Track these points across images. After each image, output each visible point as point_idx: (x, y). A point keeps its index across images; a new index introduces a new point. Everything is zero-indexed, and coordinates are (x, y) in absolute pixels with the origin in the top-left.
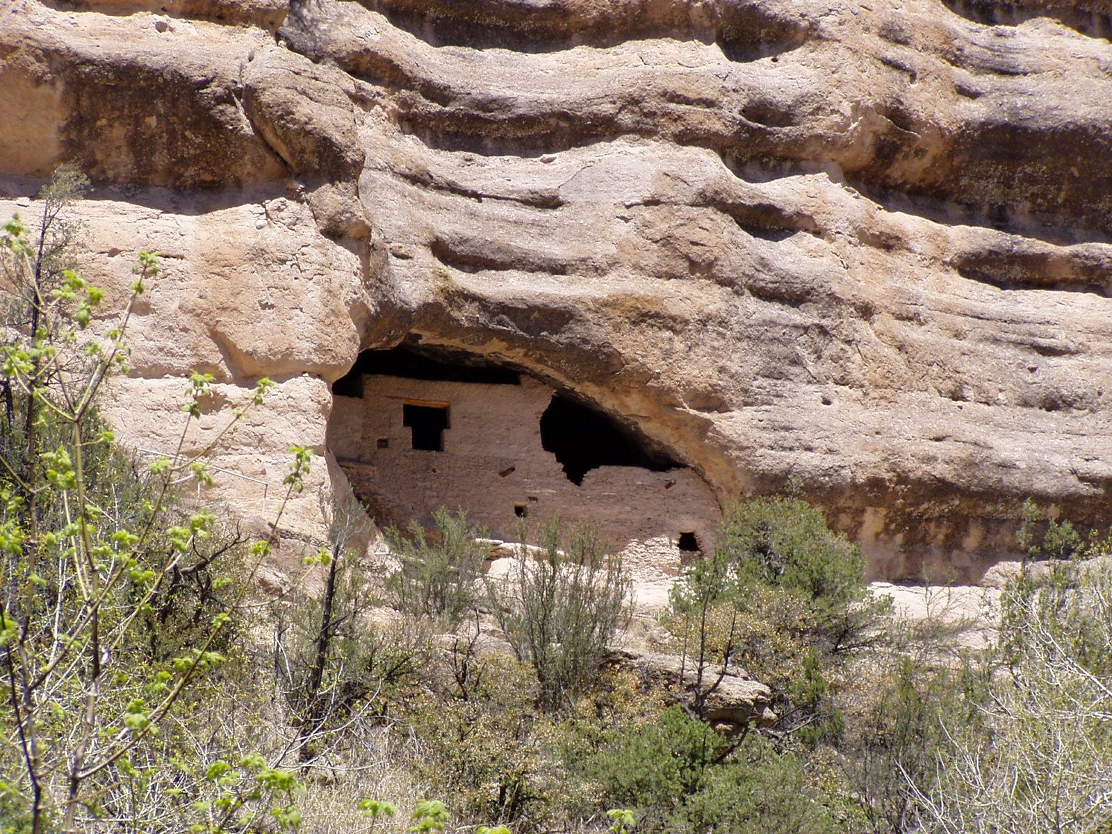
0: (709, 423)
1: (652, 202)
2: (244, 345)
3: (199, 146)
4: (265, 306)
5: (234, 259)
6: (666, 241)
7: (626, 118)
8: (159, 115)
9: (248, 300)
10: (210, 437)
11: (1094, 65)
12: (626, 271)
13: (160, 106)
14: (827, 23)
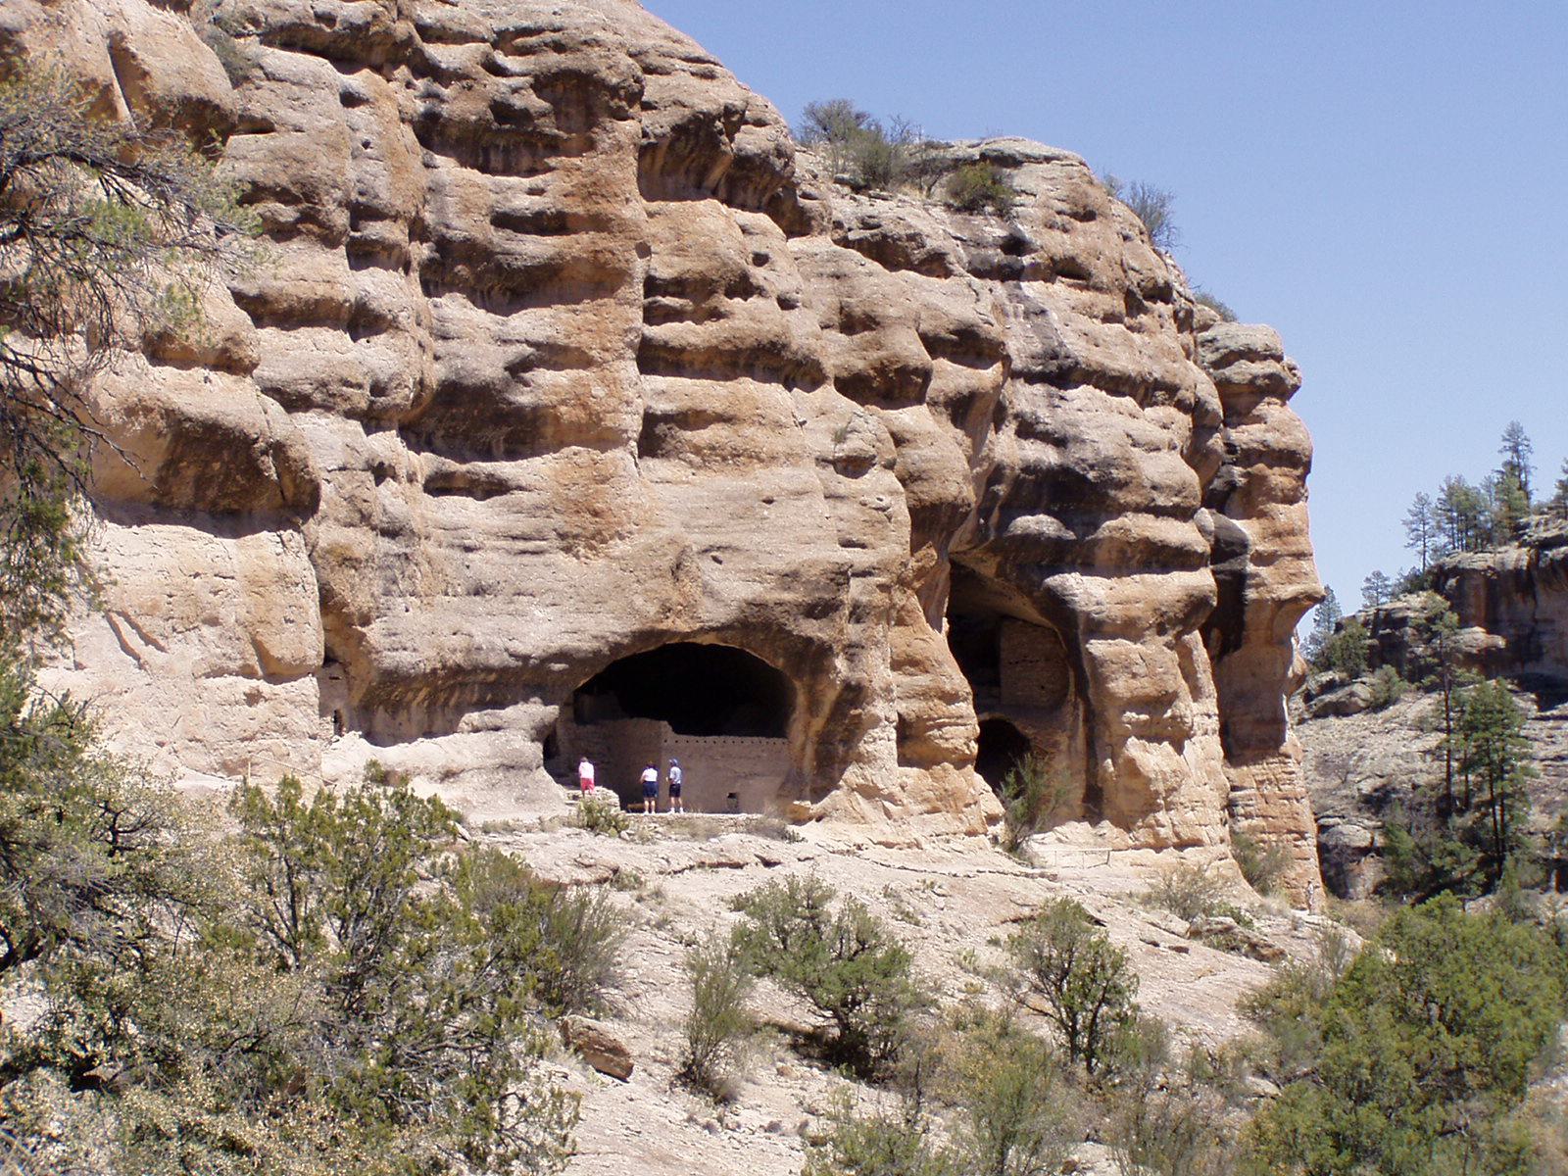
0: (364, 635)
1: (342, 469)
2: (276, 653)
3: (242, 486)
4: (287, 621)
5: (266, 581)
6: (350, 499)
7: (318, 397)
8: (223, 462)
9: (277, 615)
10: (255, 726)
12: (331, 522)
13: (226, 455)
14: (402, 317)
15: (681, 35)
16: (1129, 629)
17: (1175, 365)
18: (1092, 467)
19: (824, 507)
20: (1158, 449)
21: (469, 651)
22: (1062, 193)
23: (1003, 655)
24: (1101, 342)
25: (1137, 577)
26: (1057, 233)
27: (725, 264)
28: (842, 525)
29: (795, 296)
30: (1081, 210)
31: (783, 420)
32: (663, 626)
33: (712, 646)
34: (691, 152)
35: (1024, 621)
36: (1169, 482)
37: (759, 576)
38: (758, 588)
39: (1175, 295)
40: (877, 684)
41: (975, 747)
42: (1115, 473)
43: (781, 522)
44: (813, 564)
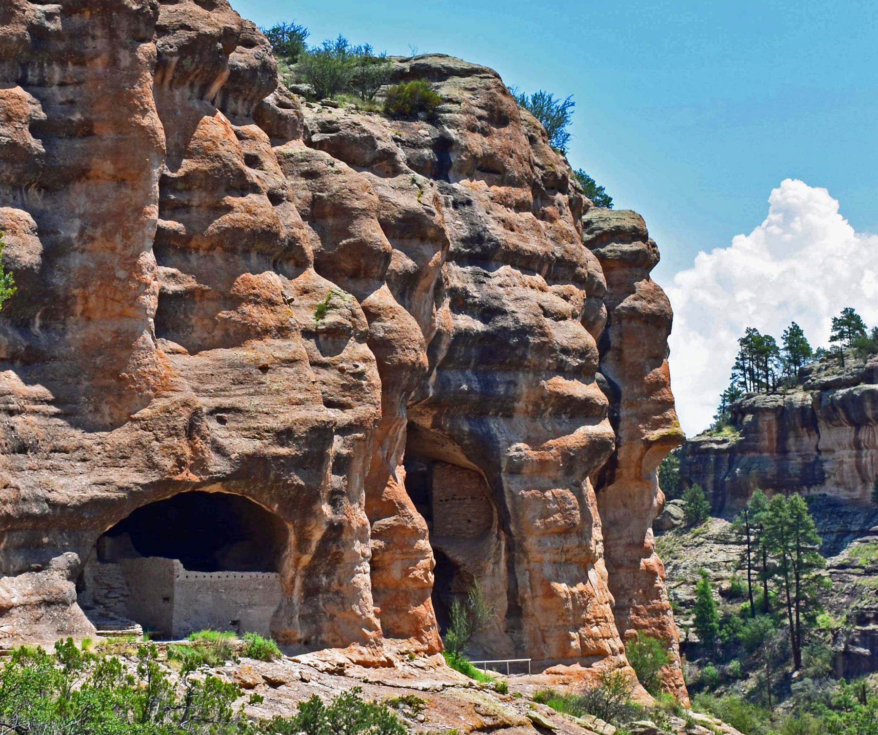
17: (573, 246)
19: (310, 373)
20: (564, 318)
21: (16, 502)
22: (481, 100)
23: (436, 493)
26: (477, 136)
27: (225, 165)
28: (324, 388)
29: (281, 191)
31: (275, 298)
32: (178, 478)
33: (218, 494)
35: (454, 465)
36: (575, 346)
37: (258, 434)
38: (258, 443)
39: (570, 186)
40: (355, 524)
41: (431, 577)
43: (275, 386)
44: (304, 422)
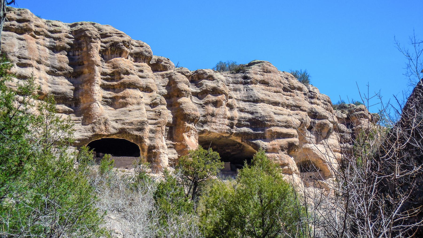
11: (66, 84)
15: (118, 30)
16: (274, 150)
18: (260, 118)
20: (282, 115)
22: (260, 68)
24: (270, 96)
25: (276, 140)
30: (266, 71)
34: (115, 50)
42: (266, 119)
